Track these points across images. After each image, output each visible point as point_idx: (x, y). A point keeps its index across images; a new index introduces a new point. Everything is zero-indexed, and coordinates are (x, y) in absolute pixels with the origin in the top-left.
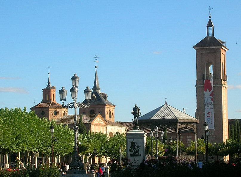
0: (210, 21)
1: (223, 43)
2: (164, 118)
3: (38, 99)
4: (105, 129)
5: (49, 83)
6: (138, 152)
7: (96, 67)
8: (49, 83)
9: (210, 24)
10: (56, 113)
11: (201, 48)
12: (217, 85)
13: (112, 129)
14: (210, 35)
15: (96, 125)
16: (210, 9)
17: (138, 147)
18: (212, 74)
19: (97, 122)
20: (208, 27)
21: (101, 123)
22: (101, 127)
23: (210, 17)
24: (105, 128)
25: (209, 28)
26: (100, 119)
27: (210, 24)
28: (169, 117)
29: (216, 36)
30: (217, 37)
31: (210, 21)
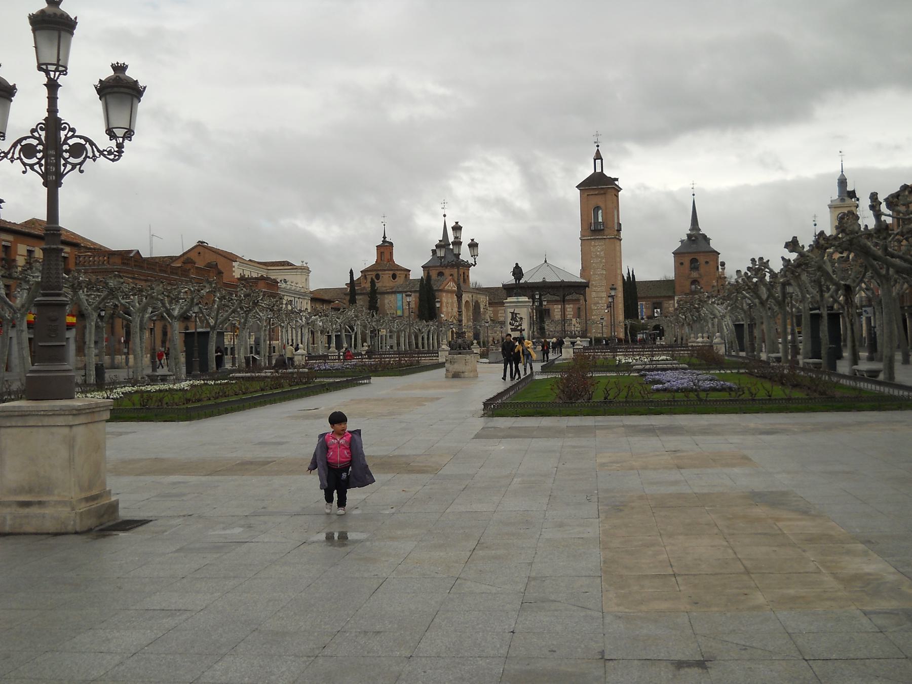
1: (617, 179)
3: (371, 259)
5: (385, 237)
6: (521, 325)
7: (445, 216)
8: (385, 237)
9: (598, 156)
10: (394, 277)
14: (599, 170)
15: (448, 291)
16: (597, 135)
17: (521, 319)
20: (595, 160)
27: (598, 156)
28: (552, 278)
30: (608, 173)
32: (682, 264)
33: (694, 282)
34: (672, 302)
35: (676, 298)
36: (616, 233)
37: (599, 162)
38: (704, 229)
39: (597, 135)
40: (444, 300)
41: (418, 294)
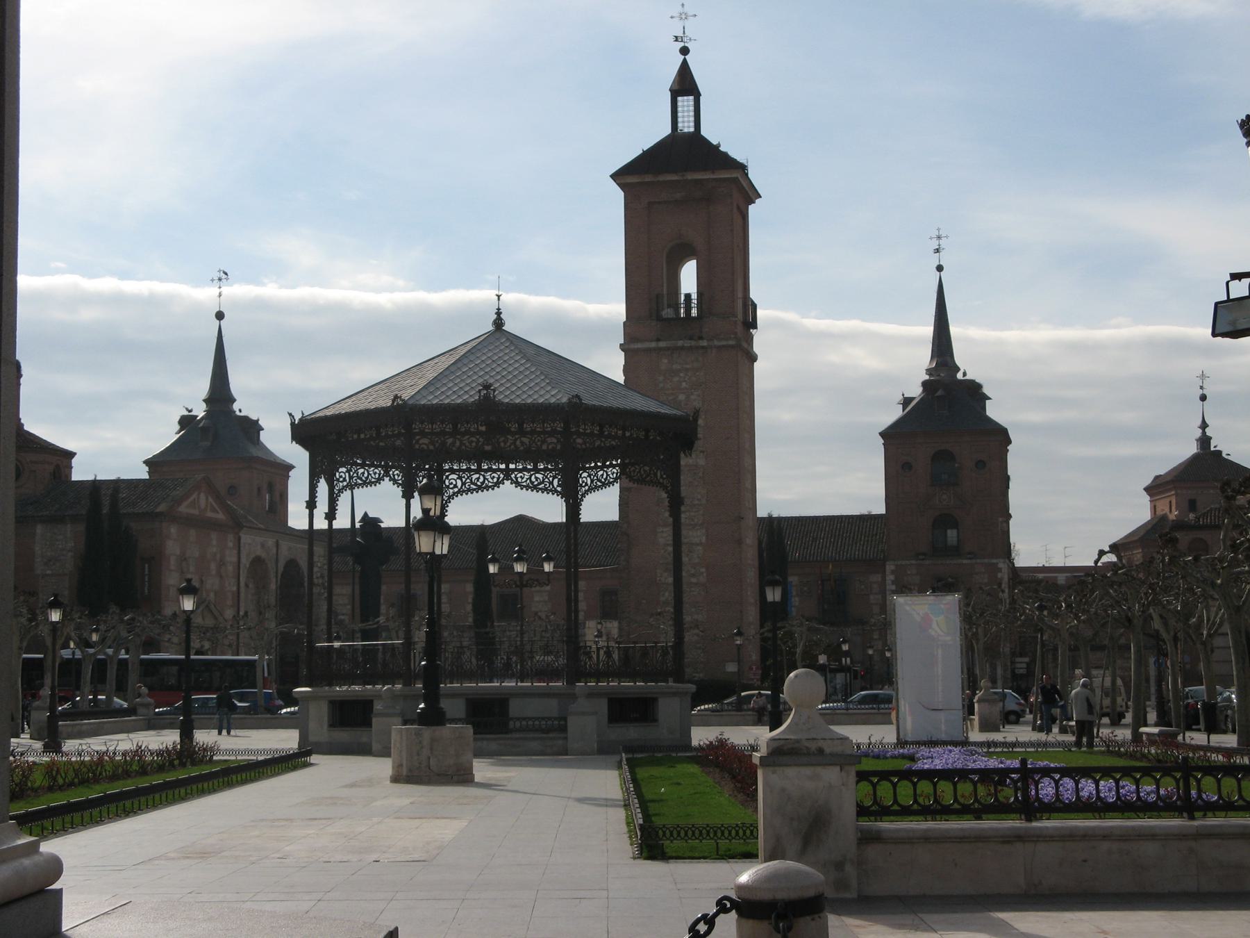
0: (685, 71)
2: (486, 397)
4: (231, 544)
9: (685, 85)
11: (648, 178)
12: (716, 343)
13: (263, 546)
14: (686, 125)
15: (190, 522)
16: (684, 16)
18: (694, 296)
19: (196, 512)
20: (676, 93)
21: (209, 514)
22: (214, 536)
23: (684, 51)
24: (231, 537)
25: (680, 98)
26: (210, 500)
27: (685, 85)
29: (705, 132)
31: (685, 71)
32: (907, 466)
33: (945, 521)
34: (876, 578)
35: (890, 567)
36: (740, 329)
37: (686, 103)
38: (968, 364)
39: (684, 16)
40: (172, 548)
41: (81, 528)
